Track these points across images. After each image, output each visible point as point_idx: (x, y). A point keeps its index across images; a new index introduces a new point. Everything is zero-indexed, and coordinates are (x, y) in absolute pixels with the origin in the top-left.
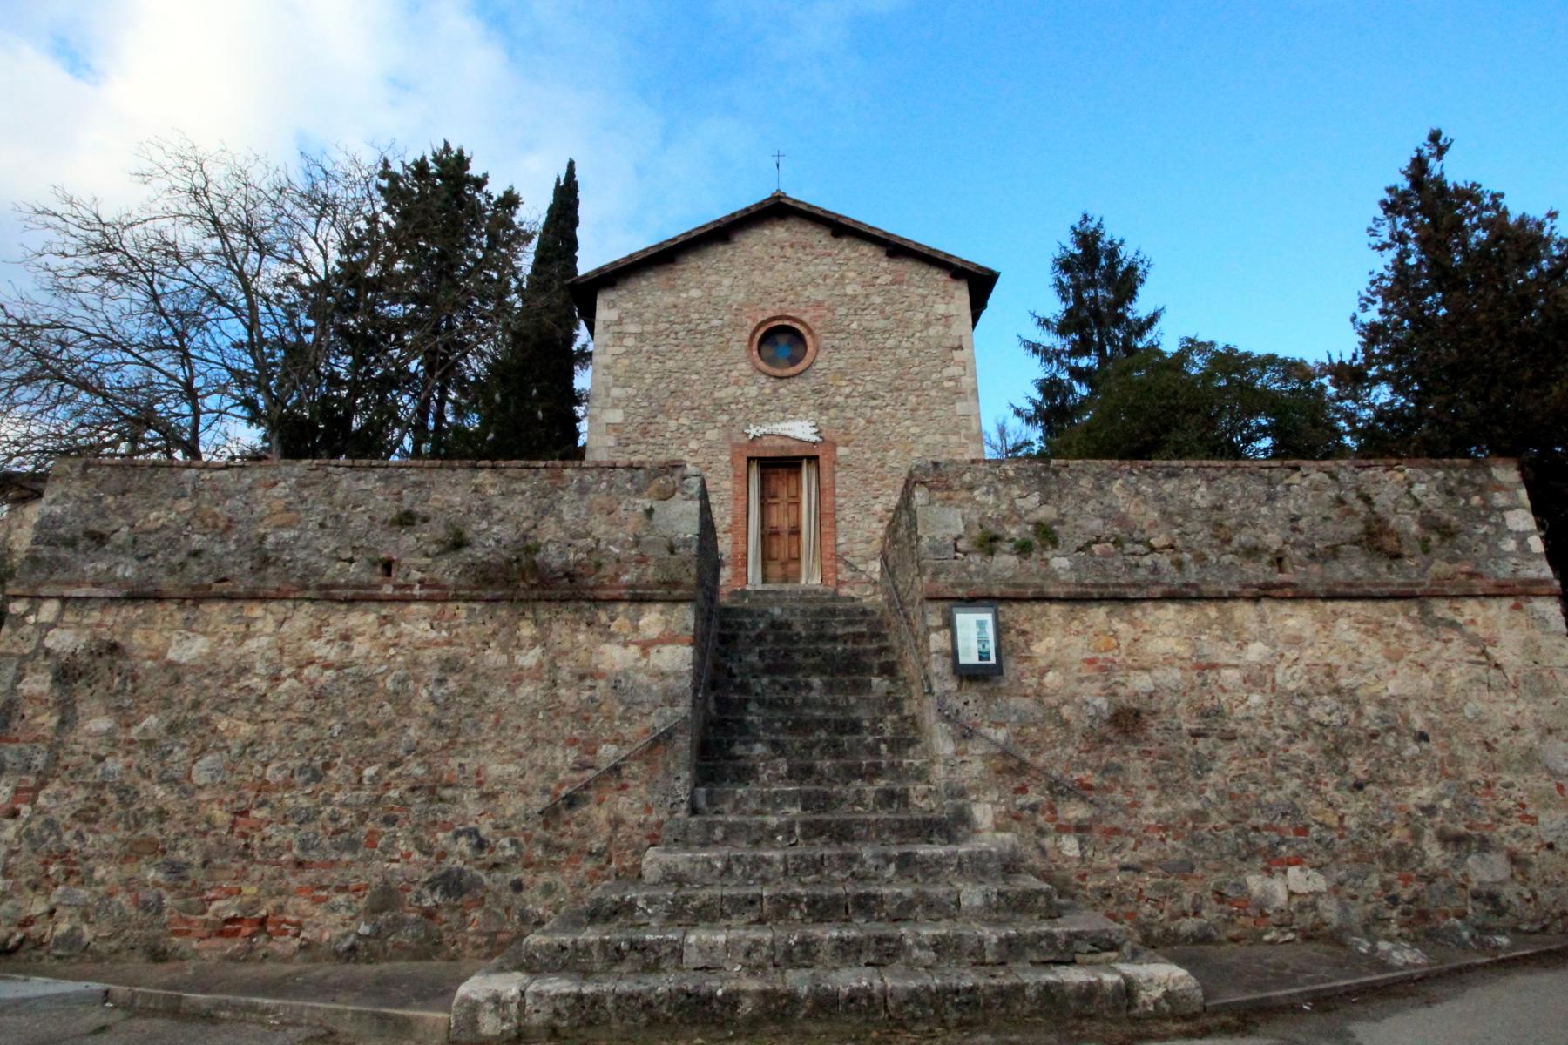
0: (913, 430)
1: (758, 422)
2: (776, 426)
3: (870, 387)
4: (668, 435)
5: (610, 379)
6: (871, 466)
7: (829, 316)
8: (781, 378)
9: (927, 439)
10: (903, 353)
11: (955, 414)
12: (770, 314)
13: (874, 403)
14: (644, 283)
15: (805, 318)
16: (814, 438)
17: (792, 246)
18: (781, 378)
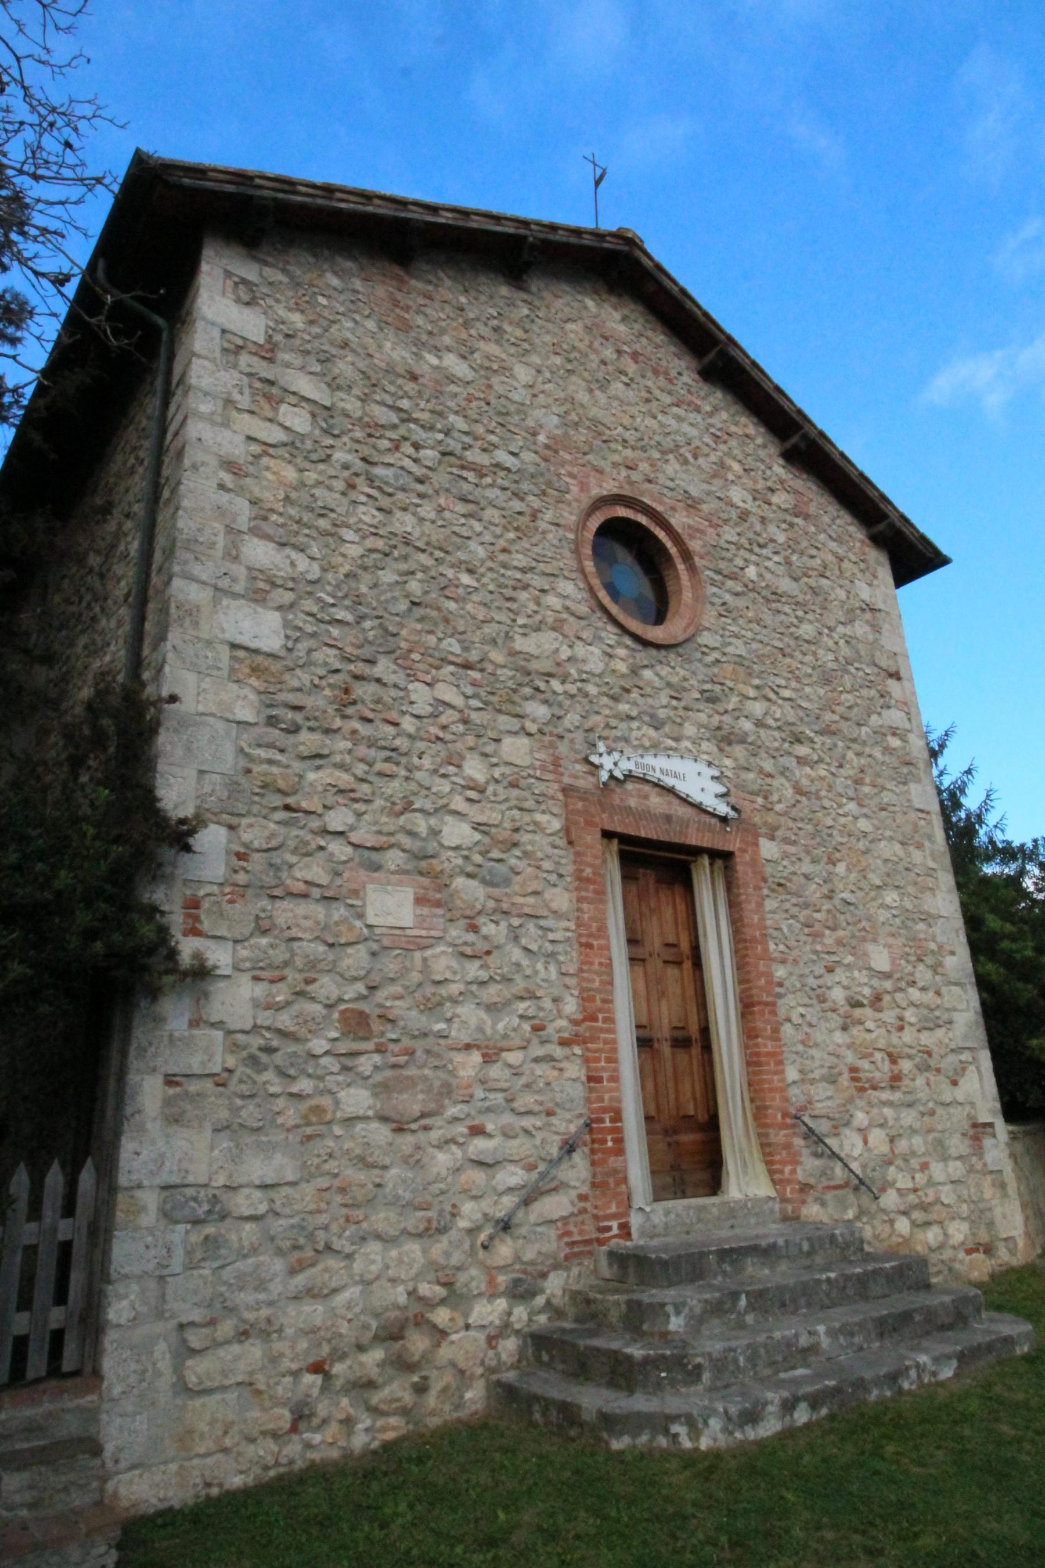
1: (618, 744)
2: (649, 760)
4: (408, 724)
5: (243, 512)
8: (646, 643)
16: (723, 809)
18: (646, 643)
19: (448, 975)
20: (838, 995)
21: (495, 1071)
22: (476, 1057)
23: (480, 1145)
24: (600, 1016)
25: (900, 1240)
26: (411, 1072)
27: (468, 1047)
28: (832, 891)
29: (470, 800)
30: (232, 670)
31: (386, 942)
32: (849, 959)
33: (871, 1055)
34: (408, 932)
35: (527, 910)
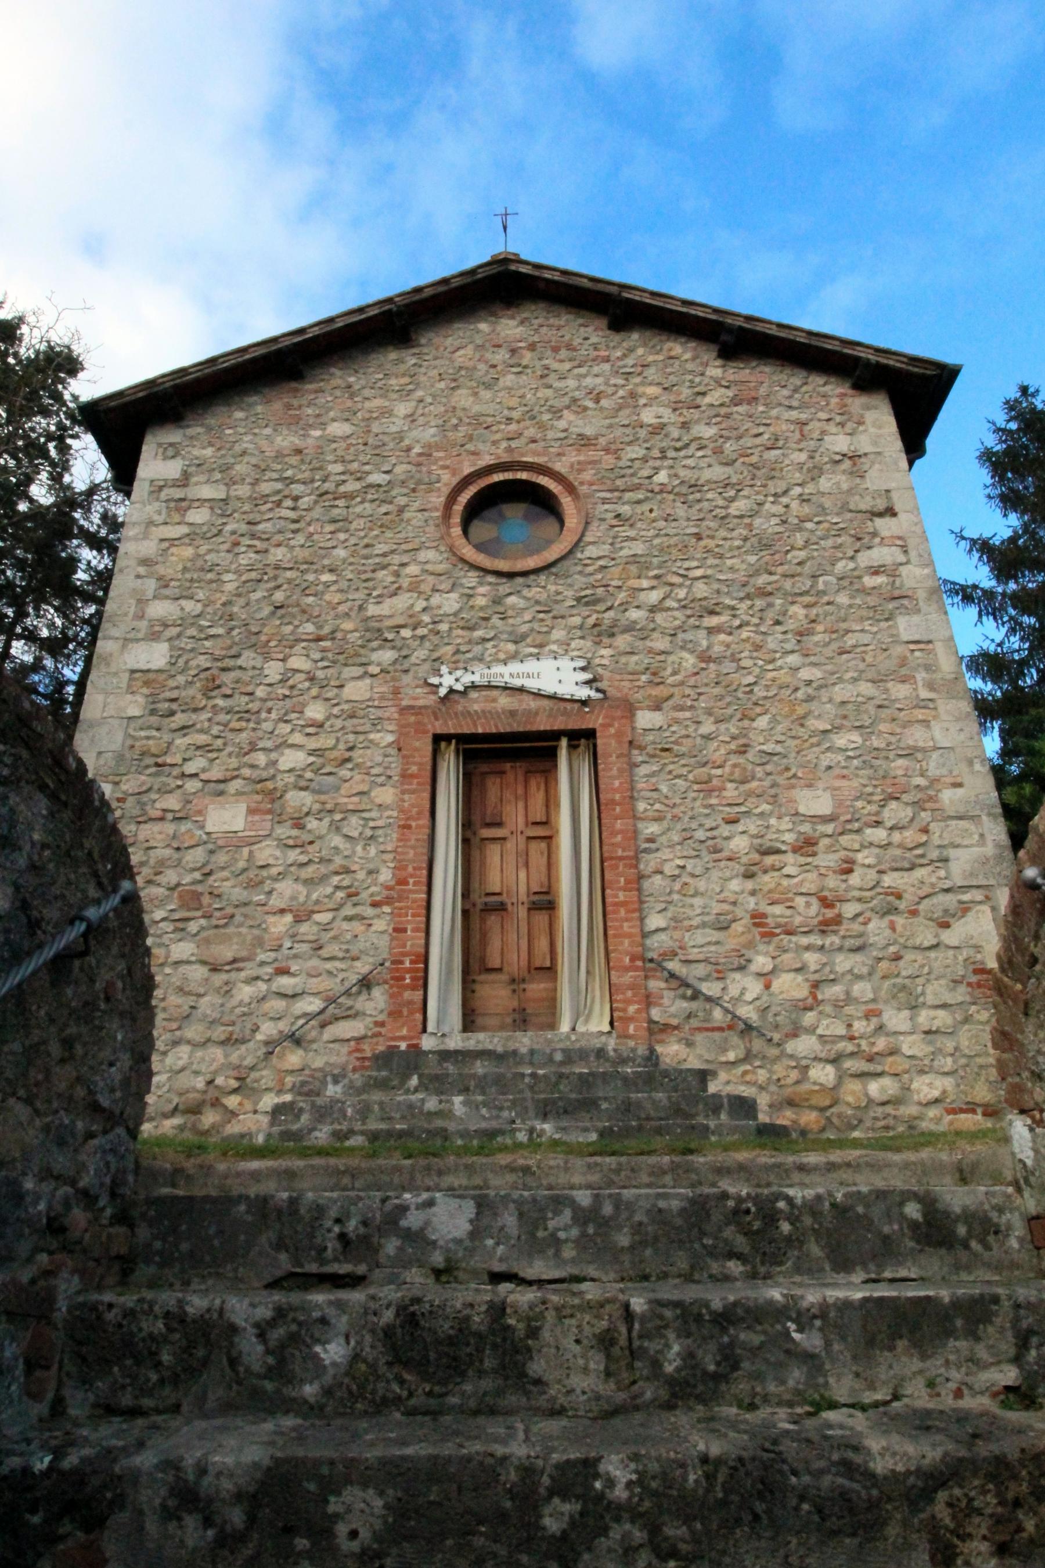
0: (805, 674)
1: (459, 661)
2: (498, 669)
3: (701, 589)
4: (261, 692)
5: (151, 585)
6: (716, 751)
7: (609, 460)
8: (511, 575)
9: (840, 692)
10: (766, 525)
11: (896, 640)
12: (487, 460)
13: (714, 621)
14: (239, 415)
15: (558, 467)
16: (584, 693)
17: (532, 347)
18: (511, 575)
19: (271, 861)
20: (740, 844)
21: (304, 928)
22: (289, 918)
23: (285, 982)
24: (411, 881)
25: (817, 1088)
26: (231, 930)
27: (282, 911)
28: (745, 745)
29: (308, 734)
30: (129, 686)
31: (220, 842)
32: (765, 807)
33: (792, 900)
34: (240, 834)
35: (350, 807)
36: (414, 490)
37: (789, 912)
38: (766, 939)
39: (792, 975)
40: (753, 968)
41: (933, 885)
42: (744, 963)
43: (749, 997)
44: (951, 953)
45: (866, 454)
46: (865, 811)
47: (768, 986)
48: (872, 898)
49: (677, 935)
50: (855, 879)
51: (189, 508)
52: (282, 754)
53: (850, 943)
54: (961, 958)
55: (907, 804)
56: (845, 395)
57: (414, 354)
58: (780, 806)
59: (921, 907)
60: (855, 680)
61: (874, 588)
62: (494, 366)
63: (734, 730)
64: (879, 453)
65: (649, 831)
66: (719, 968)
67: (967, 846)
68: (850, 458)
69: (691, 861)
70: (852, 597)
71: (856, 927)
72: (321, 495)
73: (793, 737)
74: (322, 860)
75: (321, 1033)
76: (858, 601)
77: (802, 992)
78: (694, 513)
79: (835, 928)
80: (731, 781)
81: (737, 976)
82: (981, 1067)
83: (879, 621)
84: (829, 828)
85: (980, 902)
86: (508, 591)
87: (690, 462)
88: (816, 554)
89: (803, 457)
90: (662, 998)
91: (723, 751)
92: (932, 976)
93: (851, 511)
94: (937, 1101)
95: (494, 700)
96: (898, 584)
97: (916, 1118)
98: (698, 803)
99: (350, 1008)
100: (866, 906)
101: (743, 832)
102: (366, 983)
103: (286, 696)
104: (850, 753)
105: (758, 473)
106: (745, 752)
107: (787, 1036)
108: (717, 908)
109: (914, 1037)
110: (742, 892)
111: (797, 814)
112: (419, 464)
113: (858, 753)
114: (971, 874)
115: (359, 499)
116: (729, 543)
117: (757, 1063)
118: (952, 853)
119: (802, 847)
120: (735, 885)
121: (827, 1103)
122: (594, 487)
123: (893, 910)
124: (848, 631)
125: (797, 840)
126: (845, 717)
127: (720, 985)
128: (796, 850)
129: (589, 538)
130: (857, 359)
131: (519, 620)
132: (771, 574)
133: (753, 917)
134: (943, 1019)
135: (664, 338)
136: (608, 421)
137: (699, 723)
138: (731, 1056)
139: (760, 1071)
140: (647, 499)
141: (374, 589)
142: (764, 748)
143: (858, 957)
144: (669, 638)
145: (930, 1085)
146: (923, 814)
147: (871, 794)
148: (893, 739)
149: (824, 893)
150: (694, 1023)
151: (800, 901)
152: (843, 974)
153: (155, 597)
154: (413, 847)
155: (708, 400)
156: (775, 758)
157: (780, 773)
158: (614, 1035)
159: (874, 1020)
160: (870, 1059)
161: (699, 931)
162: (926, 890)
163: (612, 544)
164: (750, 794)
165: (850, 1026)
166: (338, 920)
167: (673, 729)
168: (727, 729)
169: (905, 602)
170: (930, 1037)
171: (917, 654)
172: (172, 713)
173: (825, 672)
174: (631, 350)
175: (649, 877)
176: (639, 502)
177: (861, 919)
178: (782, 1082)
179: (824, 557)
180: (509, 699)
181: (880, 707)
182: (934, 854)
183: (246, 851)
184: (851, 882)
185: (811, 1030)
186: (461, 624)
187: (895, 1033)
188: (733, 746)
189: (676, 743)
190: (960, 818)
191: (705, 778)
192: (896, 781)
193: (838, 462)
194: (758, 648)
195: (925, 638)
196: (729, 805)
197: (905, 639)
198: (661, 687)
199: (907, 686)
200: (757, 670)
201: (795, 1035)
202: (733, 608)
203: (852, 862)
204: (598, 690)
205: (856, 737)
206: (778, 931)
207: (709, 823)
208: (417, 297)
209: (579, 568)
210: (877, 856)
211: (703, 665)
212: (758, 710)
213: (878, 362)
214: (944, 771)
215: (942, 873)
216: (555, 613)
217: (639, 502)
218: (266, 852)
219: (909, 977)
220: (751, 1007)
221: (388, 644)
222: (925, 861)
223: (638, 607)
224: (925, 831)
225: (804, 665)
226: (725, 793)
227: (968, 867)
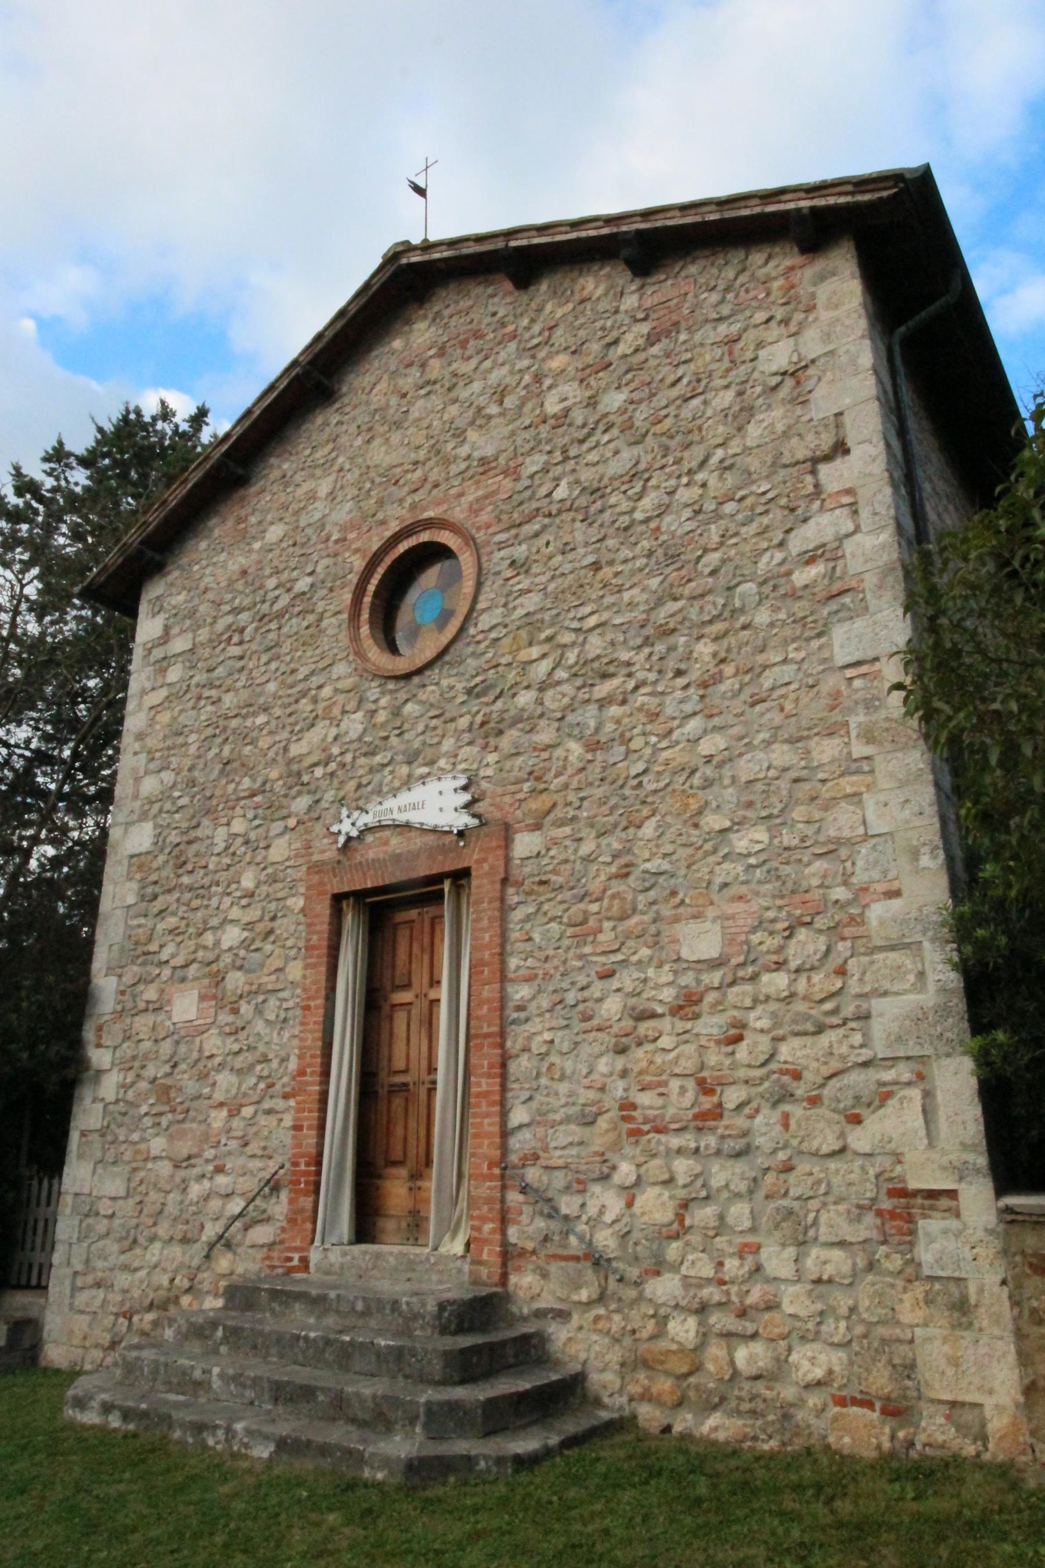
0: (705, 747)
3: (595, 645)
6: (595, 882)
7: (507, 484)
9: (747, 768)
10: (677, 524)
11: (828, 667)
12: (394, 527)
13: (603, 689)
14: (203, 545)
15: (458, 514)
16: (464, 820)
17: (442, 352)
19: (214, 1052)
20: (612, 1007)
21: (236, 1123)
22: (224, 1113)
23: (221, 1180)
24: (308, 1070)
25: (674, 1347)
26: (186, 1125)
27: (221, 1104)
28: (627, 865)
29: (244, 907)
30: (129, 873)
31: (183, 1033)
32: (645, 952)
33: (665, 1084)
34: (195, 1023)
35: (270, 987)
36: (331, 590)
37: (660, 1102)
38: (632, 1139)
39: (657, 1190)
40: (617, 1178)
41: (843, 1058)
42: (606, 1170)
43: (608, 1218)
44: (859, 1162)
45: (813, 361)
46: (764, 948)
47: (630, 1204)
48: (762, 1080)
49: (540, 1131)
50: (742, 1051)
51: (169, 666)
52: (224, 932)
53: (730, 1145)
54: (872, 1172)
55: (820, 931)
56: (792, 269)
57: (337, 410)
58: (662, 948)
59: (826, 1092)
60: (768, 743)
61: (806, 586)
62: (404, 396)
63: (616, 845)
64: (832, 353)
65: (518, 996)
66: (582, 1177)
67: (897, 994)
68: (793, 374)
69: (560, 1033)
70: (776, 609)
71: (740, 1122)
72: (261, 620)
73: (684, 845)
74: (249, 1048)
75: (245, 1236)
76: (782, 616)
77: (664, 1215)
78: (594, 533)
79: (712, 1123)
80: (609, 919)
81: (596, 1189)
82: (884, 1341)
83: (809, 639)
84: (715, 978)
85: (909, 1084)
86: (405, 697)
87: (593, 457)
88: (733, 552)
89: (728, 396)
90: (521, 1213)
91: (603, 878)
92: (830, 1199)
93: (786, 466)
94: (819, 1383)
95: (386, 843)
96: (838, 572)
97: (792, 1405)
98: (571, 954)
99: (264, 1211)
100: (754, 1091)
101: (618, 990)
102: (274, 1186)
103: (229, 866)
104: (752, 861)
105: (673, 444)
106: (627, 875)
107: (647, 1272)
108: (586, 1095)
109: (798, 1288)
110: (611, 1074)
111: (678, 959)
112: (336, 555)
113: (763, 857)
114: (899, 1039)
115: (287, 616)
116: (630, 565)
117: (613, 1307)
118: (877, 1005)
119: (681, 1008)
120: (603, 1066)
121: (685, 1369)
122: (492, 530)
123: (786, 1096)
124: (765, 667)
125: (677, 997)
126: (750, 805)
127: (578, 1200)
128: (676, 1010)
129: (480, 606)
130: (784, 215)
131: (413, 733)
132: (675, 599)
133: (622, 1108)
134: (838, 1262)
135: (576, 273)
136: (510, 428)
137: (580, 839)
138: (584, 1295)
139: (617, 1318)
140: (544, 528)
141: (296, 723)
142: (648, 866)
143: (740, 1167)
144: (556, 725)
145: (813, 1360)
146: (841, 946)
147: (774, 921)
148: (810, 830)
149: (705, 1074)
150: (551, 1249)
151: (675, 1084)
152: (719, 1190)
153: (146, 773)
154: (311, 1032)
155: (622, 349)
156: (661, 879)
157: (666, 901)
158: (468, 1260)
159: (750, 1261)
160: (742, 1314)
161: (562, 1128)
162: (835, 1065)
163: (505, 605)
164: (628, 935)
165: (721, 1264)
166: (260, 1113)
167: (552, 853)
168: (609, 845)
169: (847, 599)
170: (822, 1288)
171: (857, 683)
172: (155, 897)
173: (732, 737)
174: (540, 310)
175: (518, 1056)
176: (537, 535)
177: (747, 1110)
178: (637, 1335)
179: (743, 554)
180: (399, 839)
181: (796, 781)
182: (849, 1010)
183: (198, 1040)
184: (738, 1056)
185: (675, 1268)
186: (365, 749)
187: (775, 1279)
188: (613, 869)
189: (554, 872)
190: (893, 948)
191: (580, 918)
192: (808, 896)
193: (775, 388)
194: (654, 716)
195: (870, 654)
196: (604, 953)
197: (840, 664)
198: (544, 796)
199: (836, 741)
200: (648, 751)
201: (658, 1273)
202: (629, 664)
203: (744, 1026)
204: (474, 816)
205: (761, 834)
206: (646, 1128)
207: (582, 980)
208: (320, 346)
209: (470, 649)
210: (774, 1015)
211: (589, 757)
212: (645, 812)
213: (813, 210)
214: (876, 875)
215: (857, 1038)
216: (448, 715)
217: (537, 535)
218: (213, 1043)
219: (798, 1199)
220: (610, 1231)
221: (306, 788)
222: (835, 1020)
223: (528, 687)
224: (841, 971)
225: (705, 732)
226: (601, 937)
227: (894, 1027)
